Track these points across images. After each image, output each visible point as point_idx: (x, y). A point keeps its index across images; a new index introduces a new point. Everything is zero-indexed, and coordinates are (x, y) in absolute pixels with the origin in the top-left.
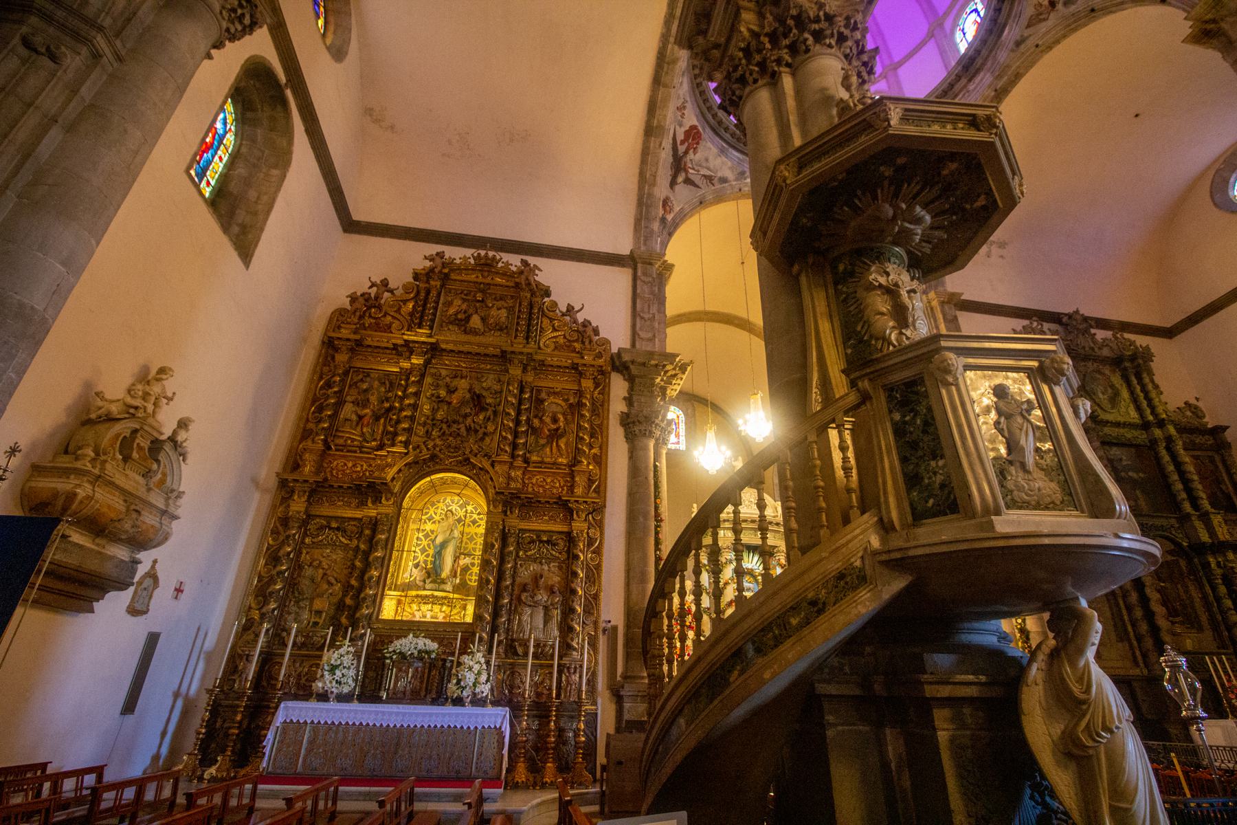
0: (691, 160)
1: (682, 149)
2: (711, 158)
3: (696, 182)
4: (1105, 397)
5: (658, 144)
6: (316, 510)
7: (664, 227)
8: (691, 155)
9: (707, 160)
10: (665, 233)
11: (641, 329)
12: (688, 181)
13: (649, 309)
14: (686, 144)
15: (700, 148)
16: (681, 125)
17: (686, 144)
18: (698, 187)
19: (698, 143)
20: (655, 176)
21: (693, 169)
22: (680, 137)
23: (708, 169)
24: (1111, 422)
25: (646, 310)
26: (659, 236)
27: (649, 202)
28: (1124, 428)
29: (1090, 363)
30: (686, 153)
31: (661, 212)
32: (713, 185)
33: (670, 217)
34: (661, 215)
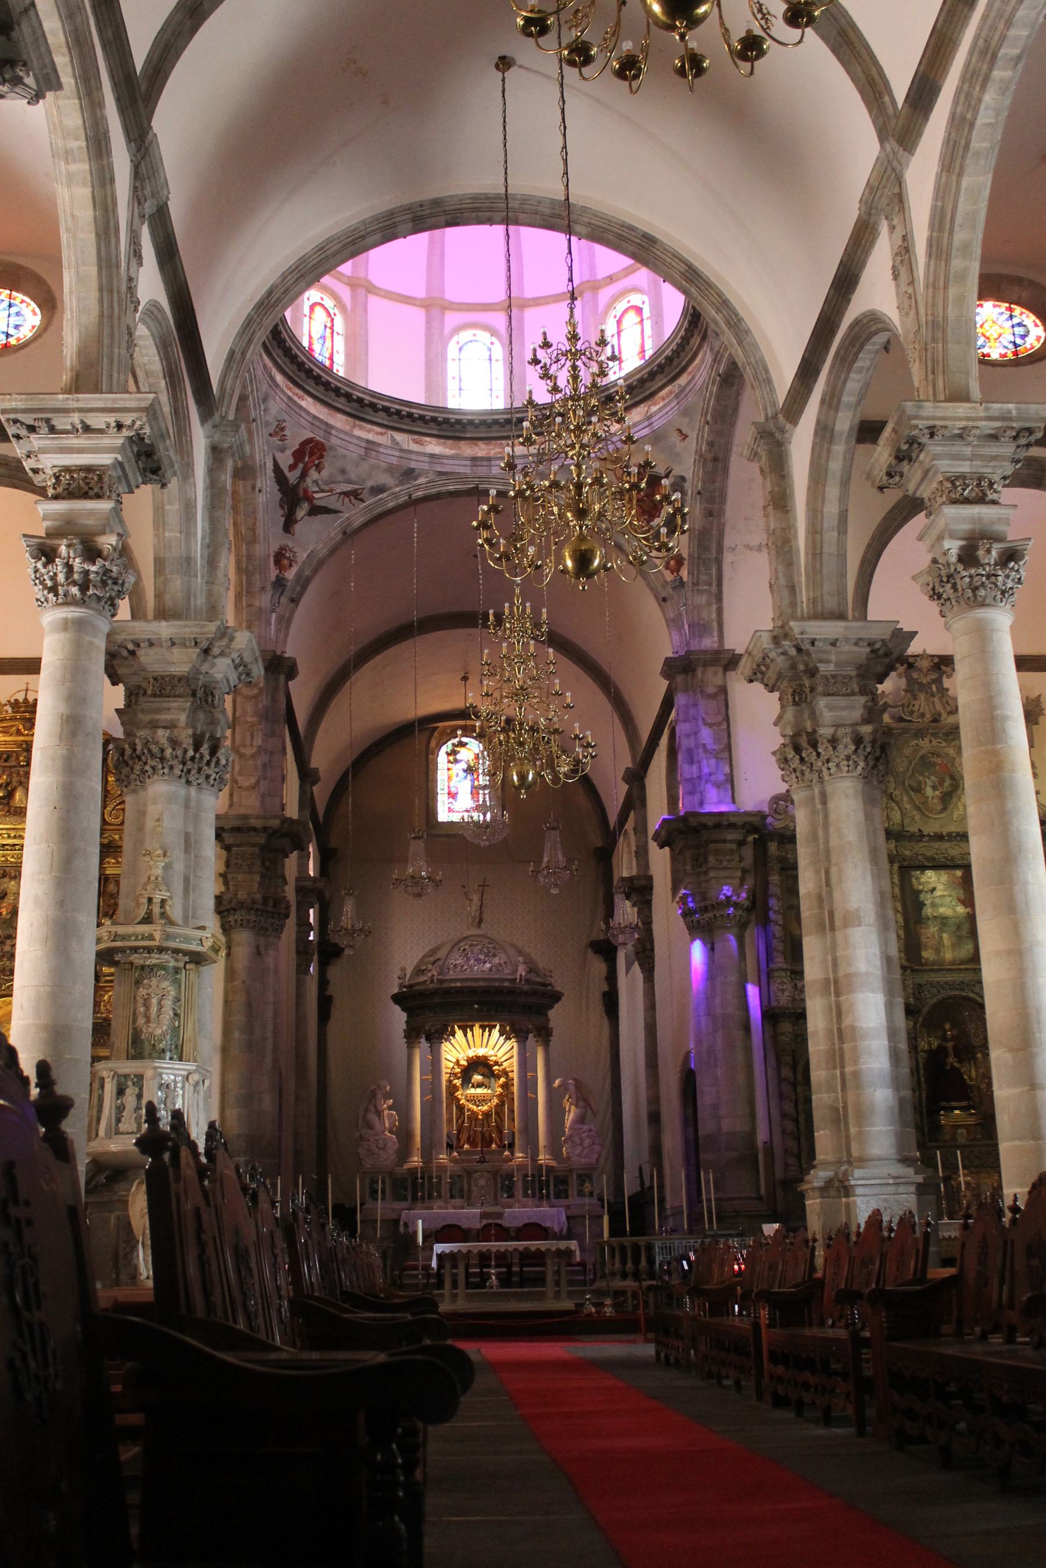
0: (316, 482)
1: (292, 477)
2: (349, 467)
3: (330, 506)
4: (937, 793)
5: (249, 488)
7: (282, 593)
8: (313, 474)
9: (343, 471)
11: (240, 773)
12: (316, 511)
13: (252, 738)
14: (301, 466)
15: (327, 462)
16: (282, 450)
17: (301, 466)
19: (322, 457)
20: (254, 530)
21: (322, 491)
22: (286, 460)
23: (349, 482)
24: (929, 835)
25: (248, 742)
26: (273, 611)
27: (251, 568)
28: (950, 841)
29: (927, 740)
30: (304, 475)
31: (273, 573)
32: (363, 501)
33: (290, 574)
34: (273, 578)
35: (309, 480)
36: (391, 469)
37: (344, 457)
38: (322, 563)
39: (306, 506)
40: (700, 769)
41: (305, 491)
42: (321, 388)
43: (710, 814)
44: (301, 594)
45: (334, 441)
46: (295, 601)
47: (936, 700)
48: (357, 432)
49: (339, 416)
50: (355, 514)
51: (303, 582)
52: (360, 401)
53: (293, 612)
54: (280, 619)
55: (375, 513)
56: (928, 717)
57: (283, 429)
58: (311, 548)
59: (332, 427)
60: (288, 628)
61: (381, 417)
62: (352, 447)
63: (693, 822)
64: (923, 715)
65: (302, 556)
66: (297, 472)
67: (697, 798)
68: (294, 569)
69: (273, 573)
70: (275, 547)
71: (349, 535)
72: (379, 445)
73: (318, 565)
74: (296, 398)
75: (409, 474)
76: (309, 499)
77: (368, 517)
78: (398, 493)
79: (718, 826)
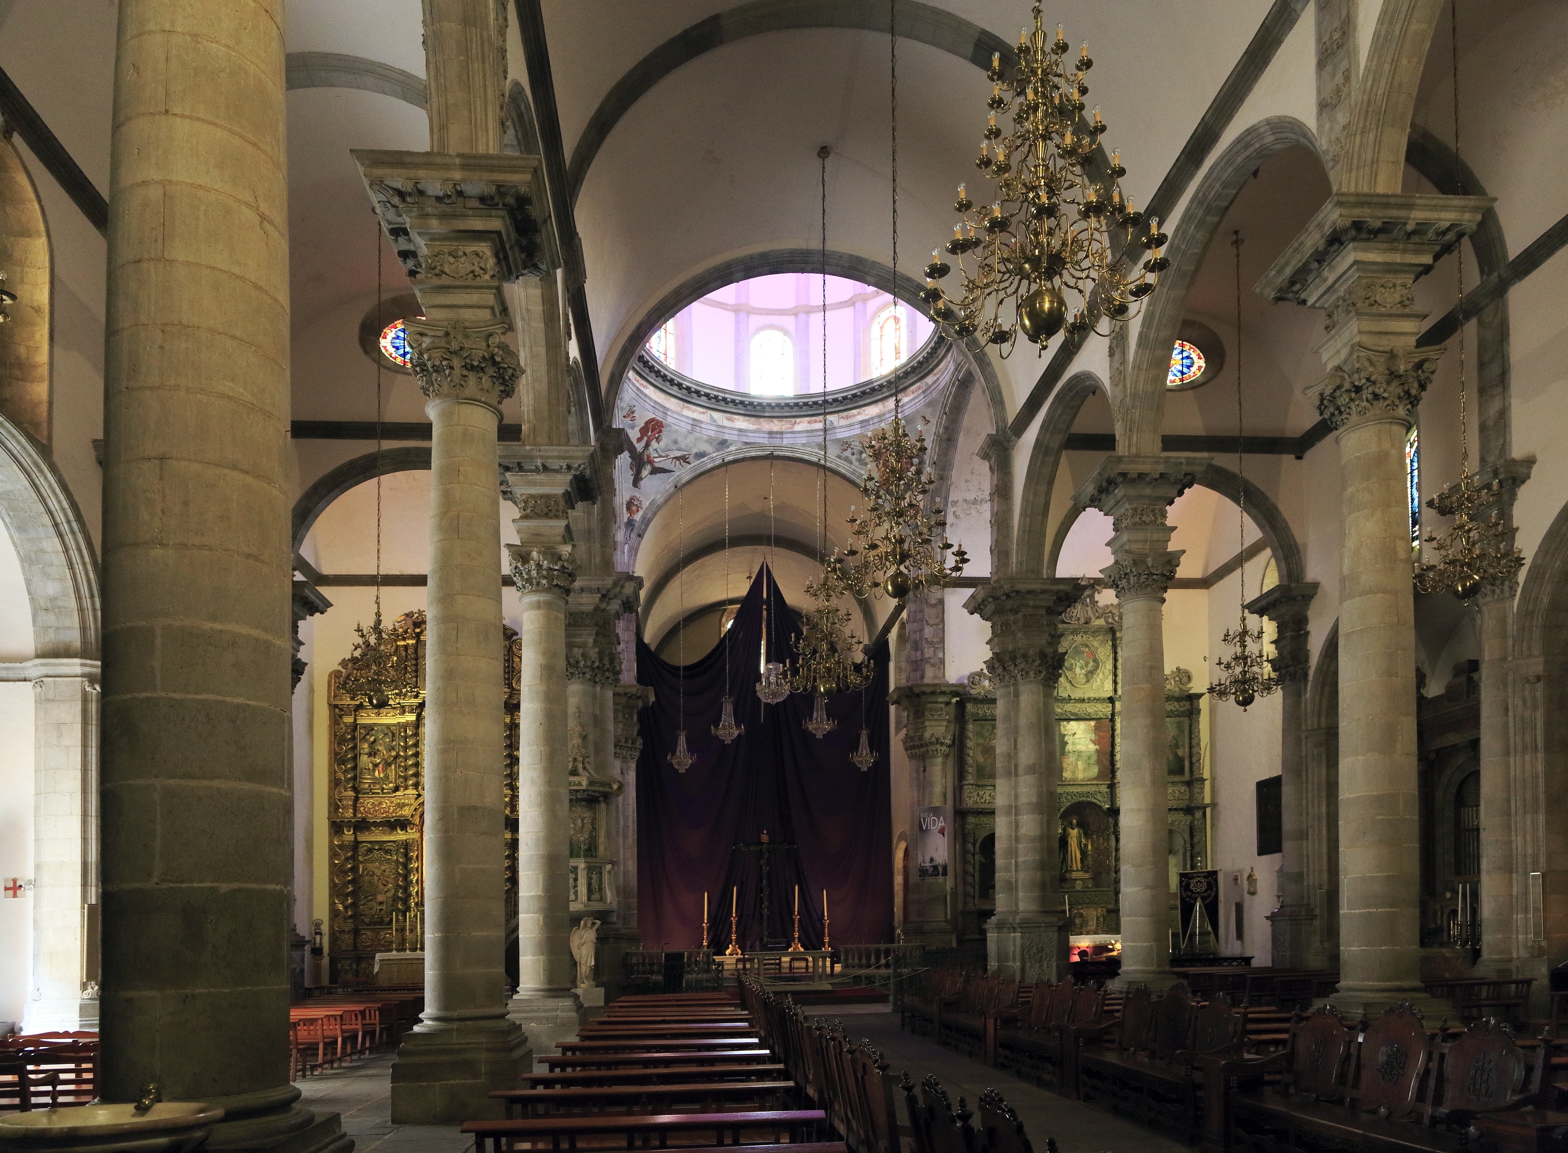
0: (656, 450)
2: (680, 439)
3: (666, 467)
6: (360, 839)
8: (654, 444)
9: (676, 442)
10: (633, 535)
12: (655, 471)
18: (670, 471)
21: (661, 456)
23: (680, 450)
30: (647, 445)
31: (626, 516)
34: (626, 520)
35: (651, 449)
36: (710, 441)
37: (677, 431)
38: (659, 508)
39: (649, 468)
40: (922, 654)
41: (648, 457)
42: (660, 379)
43: (928, 685)
44: (645, 530)
45: (670, 420)
46: (640, 536)
47: (1089, 609)
48: (686, 413)
49: (673, 400)
50: (684, 473)
51: (646, 522)
52: (688, 389)
53: (639, 544)
54: (630, 550)
55: (698, 472)
56: (1082, 621)
57: (633, 412)
58: (652, 498)
59: (668, 409)
60: (636, 555)
61: (703, 401)
62: (683, 424)
63: (917, 690)
64: (1079, 619)
65: (646, 504)
66: (643, 443)
67: (919, 674)
68: (641, 513)
69: (626, 516)
70: (626, 498)
71: (678, 488)
72: (701, 422)
73: (656, 509)
74: (642, 388)
75: (723, 443)
76: (651, 462)
77: (693, 475)
78: (715, 458)
79: (933, 693)
